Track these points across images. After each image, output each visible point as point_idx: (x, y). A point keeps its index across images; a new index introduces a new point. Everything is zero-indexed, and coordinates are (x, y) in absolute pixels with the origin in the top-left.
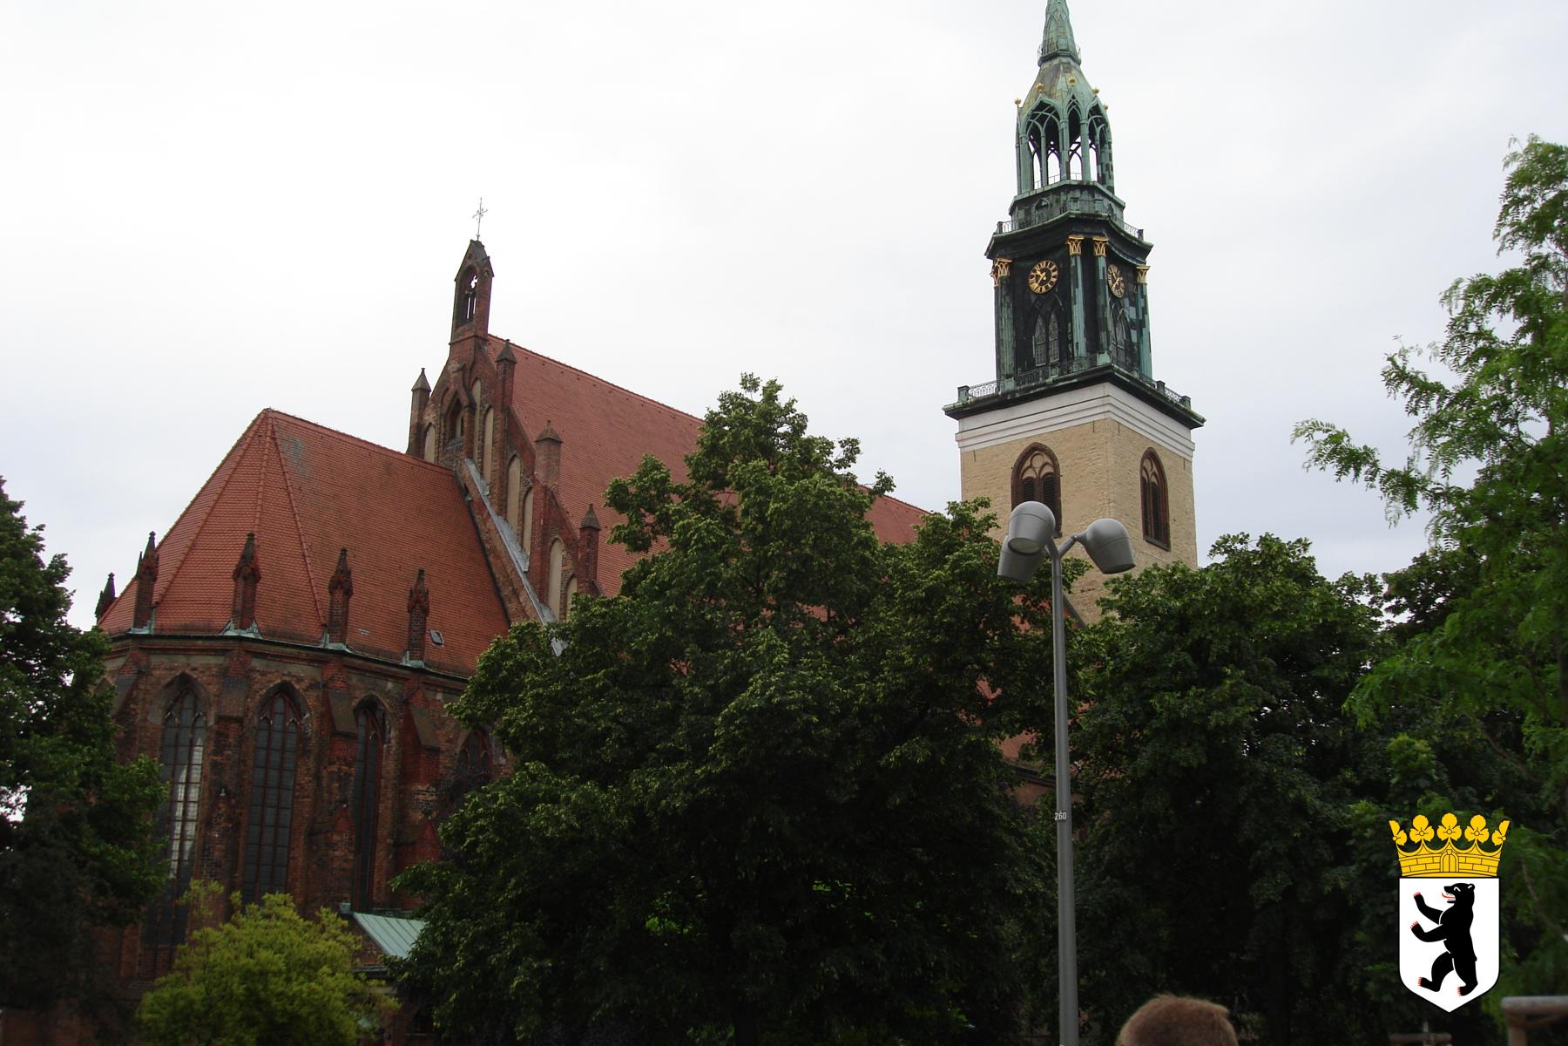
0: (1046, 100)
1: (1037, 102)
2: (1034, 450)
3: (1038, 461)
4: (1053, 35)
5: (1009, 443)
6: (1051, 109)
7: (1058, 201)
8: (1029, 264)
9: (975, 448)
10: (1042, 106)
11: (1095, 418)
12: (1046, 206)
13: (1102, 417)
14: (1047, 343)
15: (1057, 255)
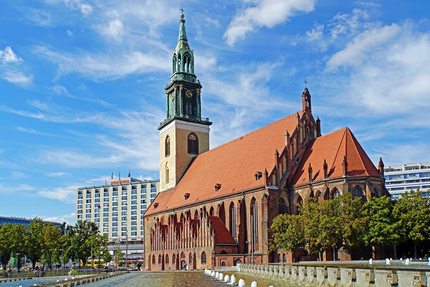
0: (188, 51)
1: (186, 51)
2: (193, 133)
3: (192, 136)
4: (184, 34)
5: (187, 130)
6: (189, 55)
7: (192, 78)
8: (185, 89)
9: (179, 128)
10: (187, 52)
11: (207, 132)
12: (189, 77)
13: (208, 132)
14: (189, 109)
15: (193, 90)
